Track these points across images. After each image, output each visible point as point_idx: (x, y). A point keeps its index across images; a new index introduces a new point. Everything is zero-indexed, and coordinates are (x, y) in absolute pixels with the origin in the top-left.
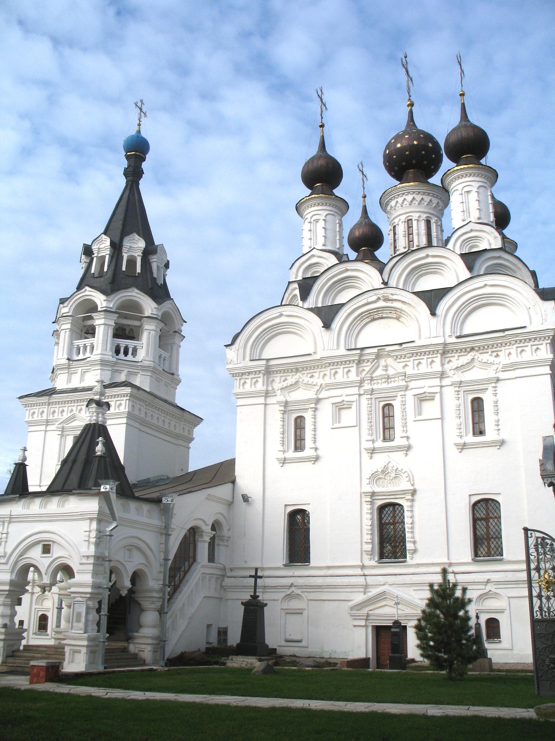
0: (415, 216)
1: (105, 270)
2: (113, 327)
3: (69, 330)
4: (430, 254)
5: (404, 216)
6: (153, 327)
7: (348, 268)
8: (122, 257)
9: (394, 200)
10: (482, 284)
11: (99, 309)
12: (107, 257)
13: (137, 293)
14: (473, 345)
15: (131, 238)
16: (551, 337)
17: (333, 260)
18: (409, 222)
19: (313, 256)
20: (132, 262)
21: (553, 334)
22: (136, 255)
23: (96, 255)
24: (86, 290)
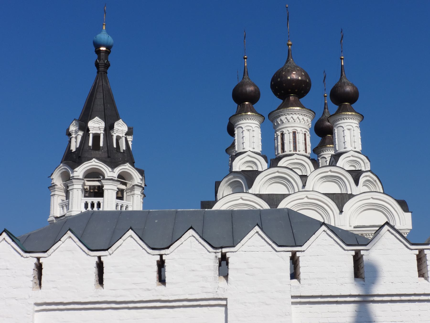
0: (299, 129)
2: (116, 191)
3: (81, 189)
4: (333, 170)
6: (139, 193)
7: (280, 171)
8: (112, 136)
9: (283, 116)
10: (370, 197)
13: (129, 167)
14: (363, 233)
15: (118, 123)
16: (408, 233)
18: (294, 133)
19: (249, 156)
21: (409, 232)
24: (94, 161)
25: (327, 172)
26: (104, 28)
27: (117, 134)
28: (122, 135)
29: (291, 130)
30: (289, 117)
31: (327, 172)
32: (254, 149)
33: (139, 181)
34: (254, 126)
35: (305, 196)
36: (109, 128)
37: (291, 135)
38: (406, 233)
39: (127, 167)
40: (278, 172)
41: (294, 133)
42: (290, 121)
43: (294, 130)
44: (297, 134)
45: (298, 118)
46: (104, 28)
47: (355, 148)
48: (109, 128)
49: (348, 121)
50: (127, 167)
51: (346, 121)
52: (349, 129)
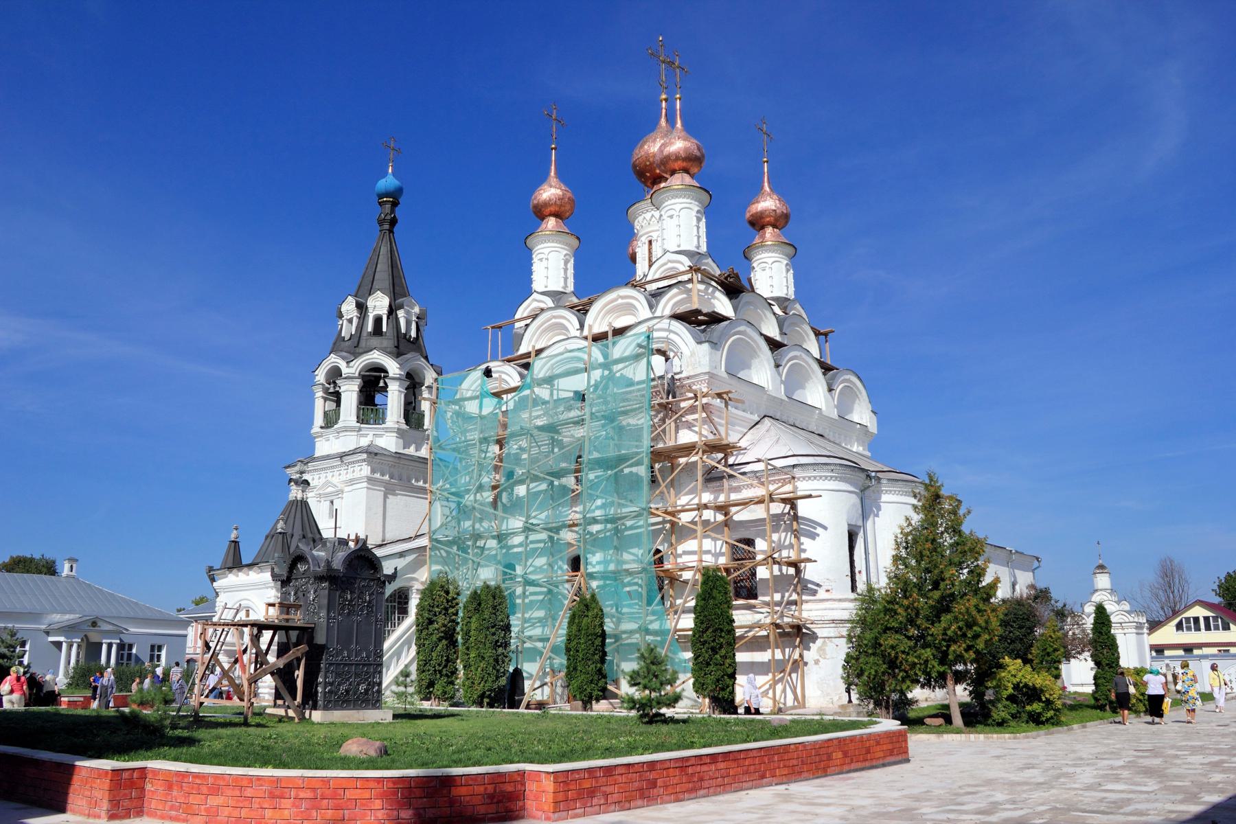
1: (353, 333)
5: (646, 236)
11: (343, 376)
12: (355, 318)
17: (551, 304)
18: (650, 242)
20: (378, 320)
22: (380, 313)
23: (345, 317)
25: (615, 300)
26: (390, 171)
27: (375, 313)
28: (383, 312)
29: (644, 239)
30: (640, 218)
31: (615, 300)
32: (546, 287)
33: (398, 371)
34: (546, 251)
35: (563, 348)
36: (362, 307)
37: (646, 246)
38: (705, 380)
39: (375, 356)
40: (555, 317)
41: (650, 242)
42: (643, 224)
43: (650, 238)
44: (653, 244)
45: (653, 216)
46: (390, 171)
47: (679, 246)
48: (362, 307)
49: (669, 202)
50: (375, 356)
51: (666, 204)
52: (671, 217)
